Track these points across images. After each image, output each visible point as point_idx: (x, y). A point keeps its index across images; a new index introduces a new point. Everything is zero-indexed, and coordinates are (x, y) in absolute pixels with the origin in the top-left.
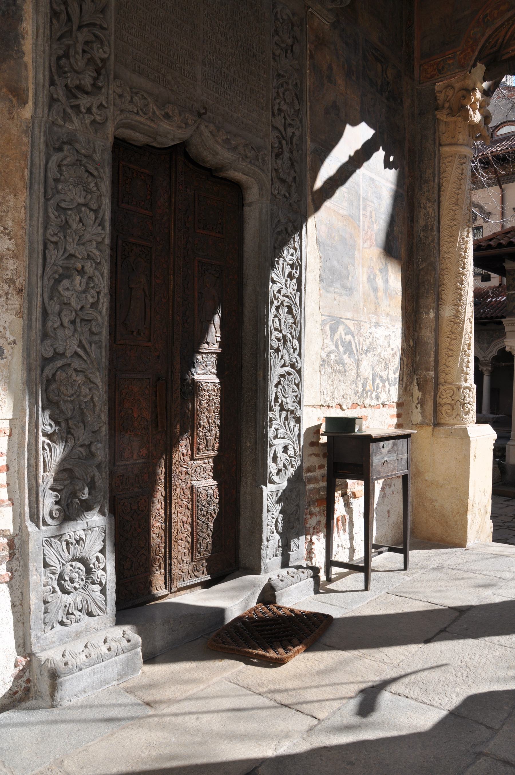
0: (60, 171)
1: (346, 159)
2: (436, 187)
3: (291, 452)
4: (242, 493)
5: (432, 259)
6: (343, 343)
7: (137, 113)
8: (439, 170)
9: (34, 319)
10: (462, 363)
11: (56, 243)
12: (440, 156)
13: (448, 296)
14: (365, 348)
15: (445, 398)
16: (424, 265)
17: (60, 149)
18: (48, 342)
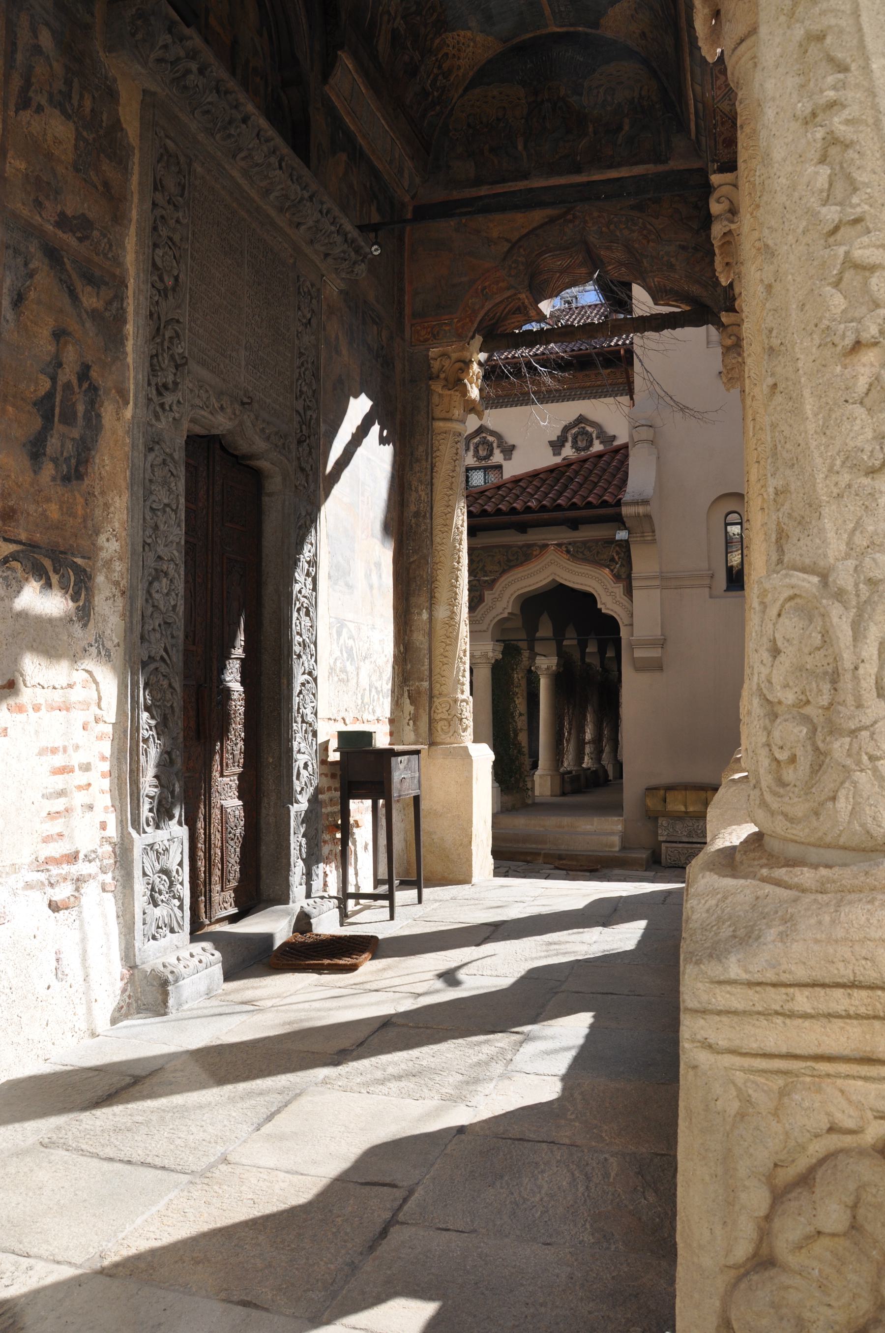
0: (153, 472)
1: (349, 438)
2: (429, 467)
3: (310, 768)
6: (346, 647)
7: (202, 408)
8: (432, 447)
9: (134, 622)
10: (458, 673)
11: (149, 545)
12: (433, 431)
13: (442, 594)
14: (364, 654)
15: (441, 713)
16: (416, 557)
17: (151, 450)
18: (146, 644)
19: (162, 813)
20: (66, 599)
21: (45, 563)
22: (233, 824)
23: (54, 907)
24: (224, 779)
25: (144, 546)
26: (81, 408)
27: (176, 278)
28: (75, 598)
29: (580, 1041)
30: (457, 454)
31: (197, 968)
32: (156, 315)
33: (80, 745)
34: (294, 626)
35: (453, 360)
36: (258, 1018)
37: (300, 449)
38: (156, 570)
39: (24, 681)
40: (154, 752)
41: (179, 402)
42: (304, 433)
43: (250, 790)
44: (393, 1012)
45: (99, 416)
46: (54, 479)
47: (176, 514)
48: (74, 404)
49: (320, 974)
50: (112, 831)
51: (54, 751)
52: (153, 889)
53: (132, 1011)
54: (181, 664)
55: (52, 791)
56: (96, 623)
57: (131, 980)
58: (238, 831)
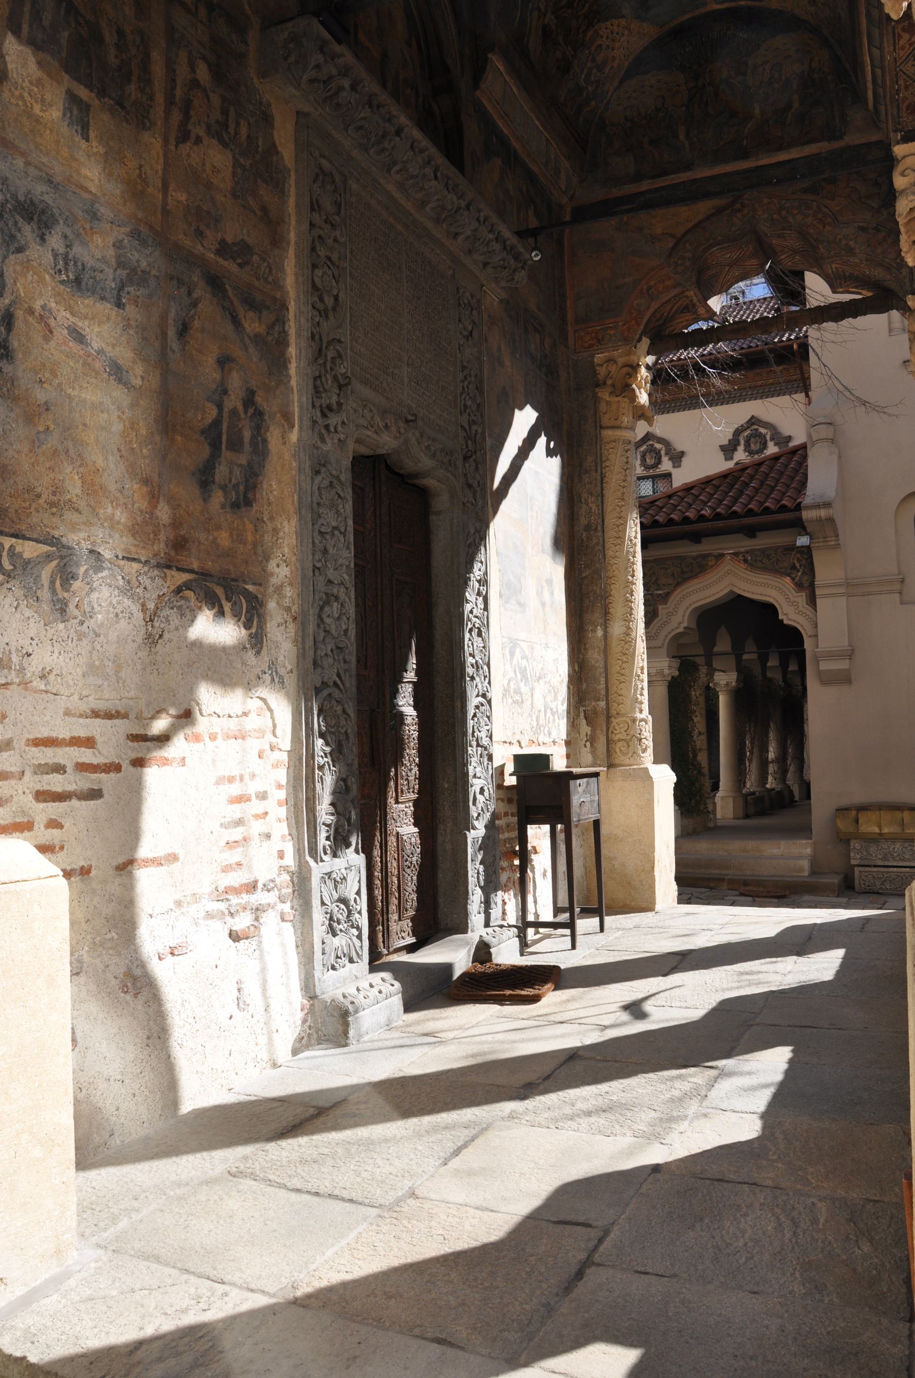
0: (320, 495)
1: (515, 451)
2: (599, 478)
3: (486, 794)
4: (439, 842)
5: (597, 565)
6: (520, 668)
7: (367, 428)
8: (601, 458)
9: (307, 648)
10: (636, 691)
11: (319, 569)
12: (601, 441)
13: (617, 609)
14: (538, 674)
15: (619, 734)
16: (588, 573)
17: (318, 472)
18: (319, 669)
19: (339, 841)
20: (239, 626)
21: (217, 591)
22: (409, 852)
23: (235, 937)
24: (400, 805)
25: (314, 571)
26: (247, 434)
27: (336, 298)
28: (247, 626)
29: (779, 1077)
30: (627, 463)
31: (377, 999)
32: (317, 337)
33: (256, 773)
34: (466, 647)
35: (620, 366)
36: (440, 1050)
37: (467, 465)
38: (326, 594)
39: (200, 710)
40: (329, 780)
41: (343, 423)
42: (470, 448)
43: (424, 817)
44: (579, 1044)
45: (265, 441)
46: (223, 506)
47: (344, 536)
48: (240, 430)
49: (502, 1005)
50: (290, 860)
51: (231, 780)
52: (331, 919)
53: (313, 1042)
54: (354, 689)
55: (230, 820)
56: (269, 650)
57: (311, 1011)
58: (415, 859)
